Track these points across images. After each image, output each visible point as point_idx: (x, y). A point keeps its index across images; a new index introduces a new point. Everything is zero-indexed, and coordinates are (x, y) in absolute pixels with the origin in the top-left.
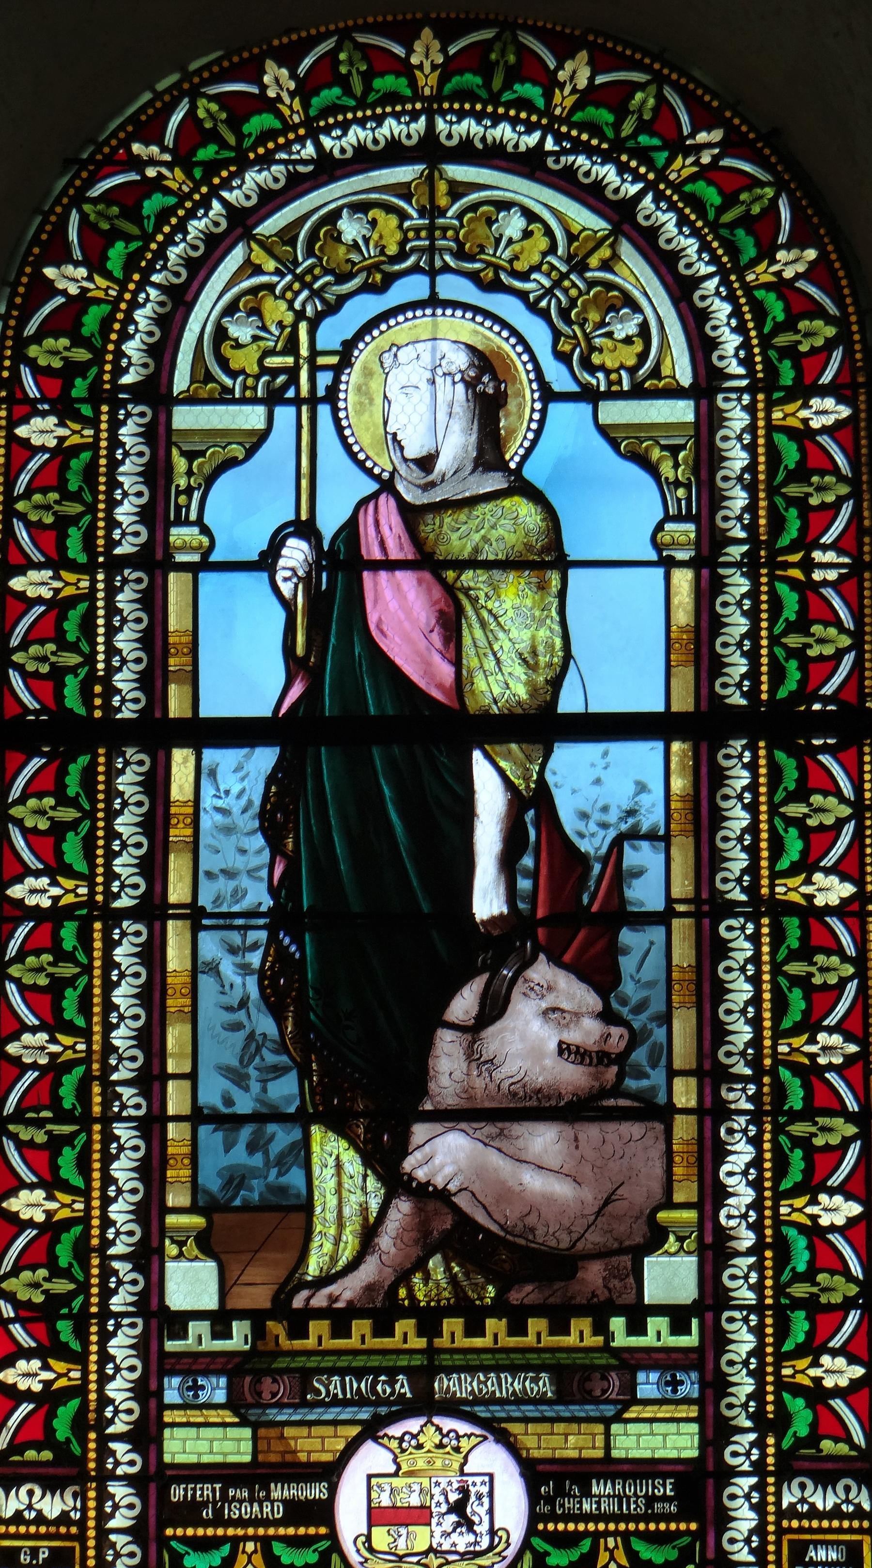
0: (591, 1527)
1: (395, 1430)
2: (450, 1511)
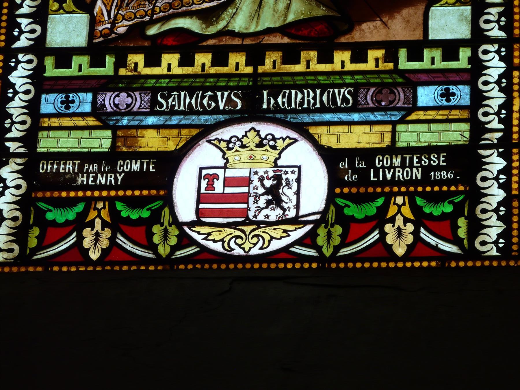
1: (226, 133)
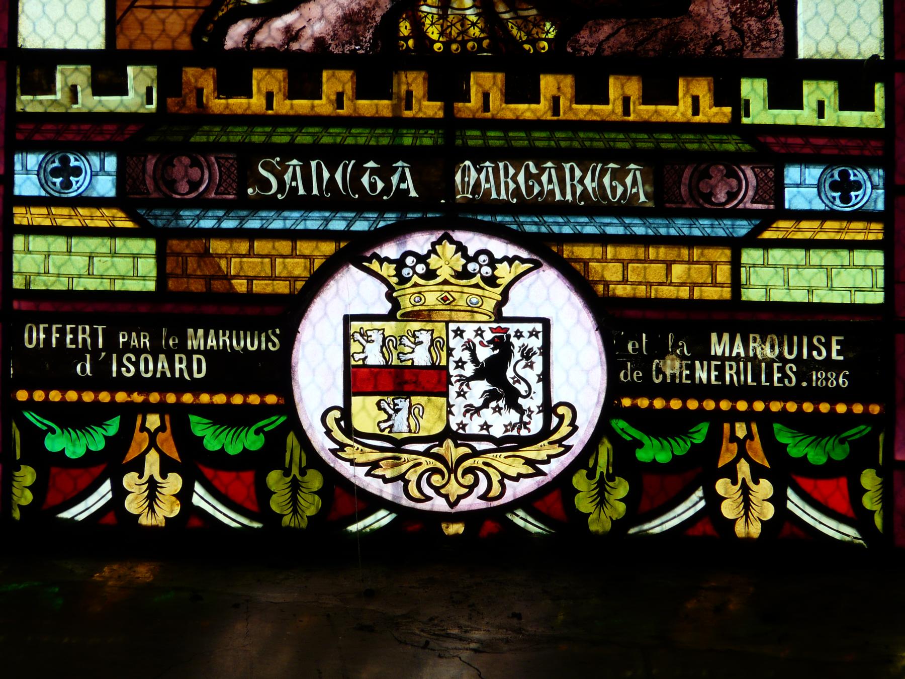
0: (710, 405)
2: (477, 376)
